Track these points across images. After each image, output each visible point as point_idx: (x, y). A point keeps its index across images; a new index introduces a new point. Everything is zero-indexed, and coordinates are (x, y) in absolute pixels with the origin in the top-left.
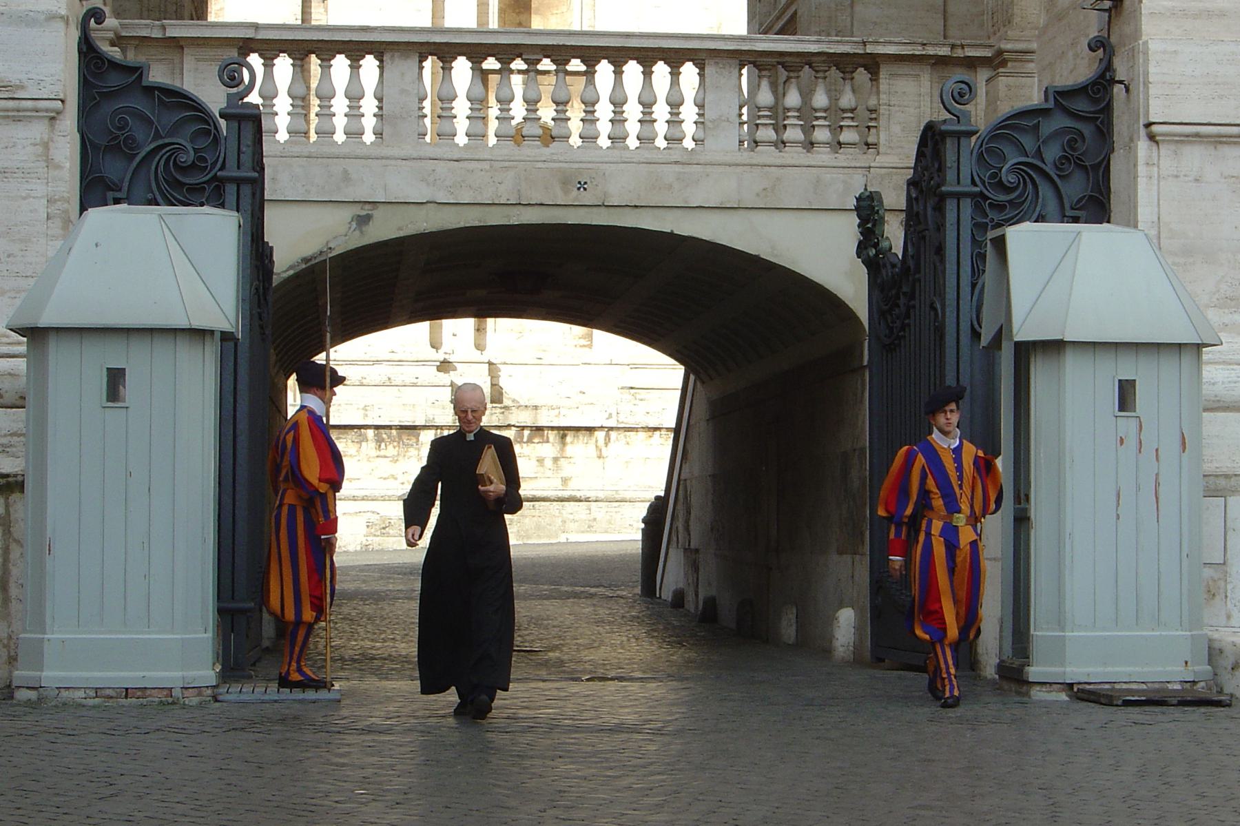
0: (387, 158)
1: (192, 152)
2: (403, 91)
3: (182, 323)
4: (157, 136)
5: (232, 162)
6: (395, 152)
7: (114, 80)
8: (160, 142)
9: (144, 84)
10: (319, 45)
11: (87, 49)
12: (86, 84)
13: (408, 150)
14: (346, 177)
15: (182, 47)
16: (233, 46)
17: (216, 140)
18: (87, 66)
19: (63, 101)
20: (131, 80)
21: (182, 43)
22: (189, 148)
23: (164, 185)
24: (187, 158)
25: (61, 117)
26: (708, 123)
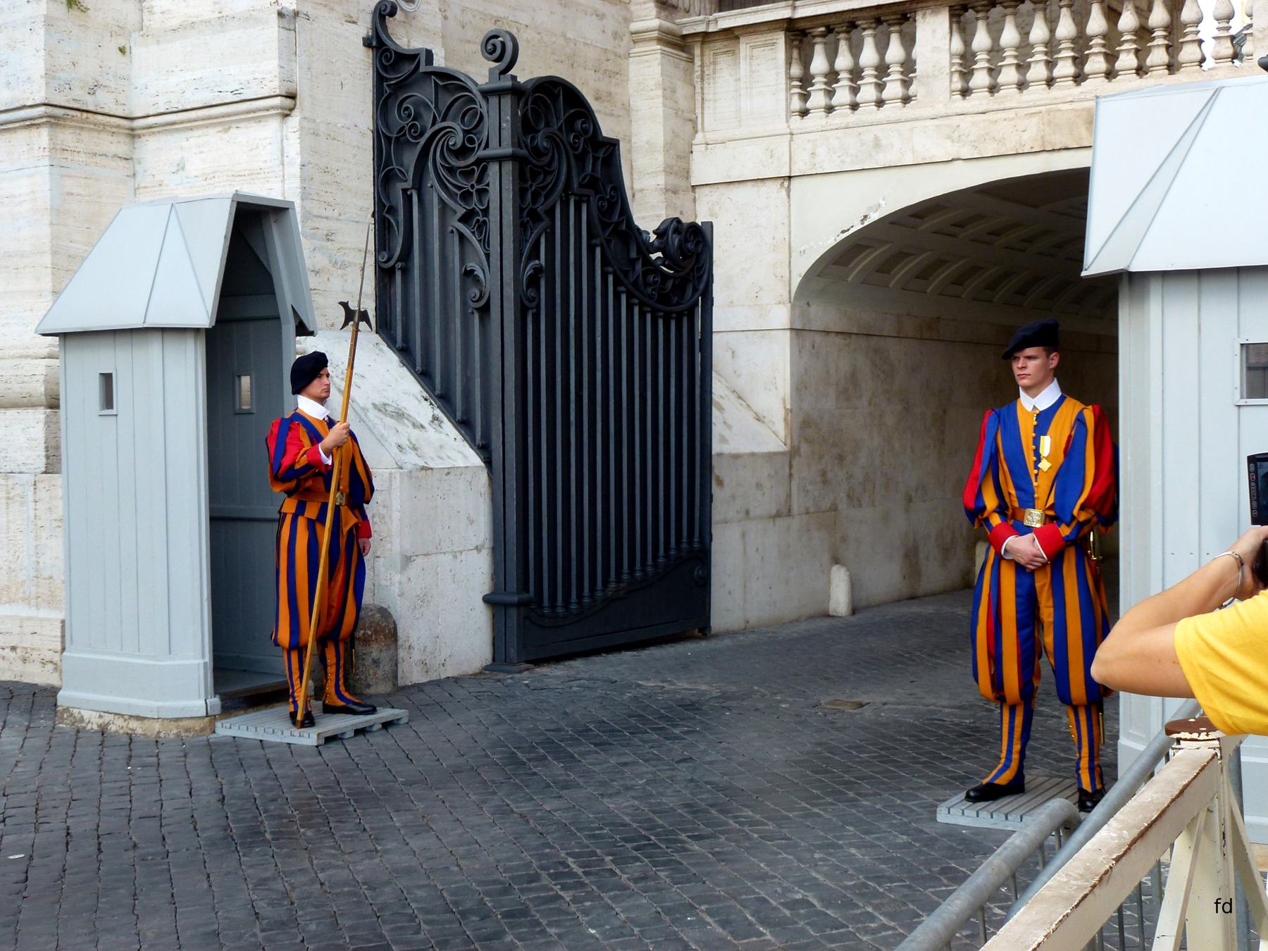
0: (917, 119)
1: (461, 134)
2: (936, 49)
3: (137, 323)
4: (434, 123)
5: (494, 142)
6: (929, 112)
7: (408, 68)
8: (436, 127)
9: (423, 68)
10: (856, 15)
11: (378, 44)
12: (379, 80)
13: (940, 109)
14: (877, 143)
15: (737, 38)
16: (775, 30)
17: (482, 117)
18: (381, 63)
19: (292, 96)
20: (413, 66)
21: (737, 33)
22: (458, 128)
23: (442, 171)
24: (457, 140)
25: (294, 113)
26: (1257, 34)
